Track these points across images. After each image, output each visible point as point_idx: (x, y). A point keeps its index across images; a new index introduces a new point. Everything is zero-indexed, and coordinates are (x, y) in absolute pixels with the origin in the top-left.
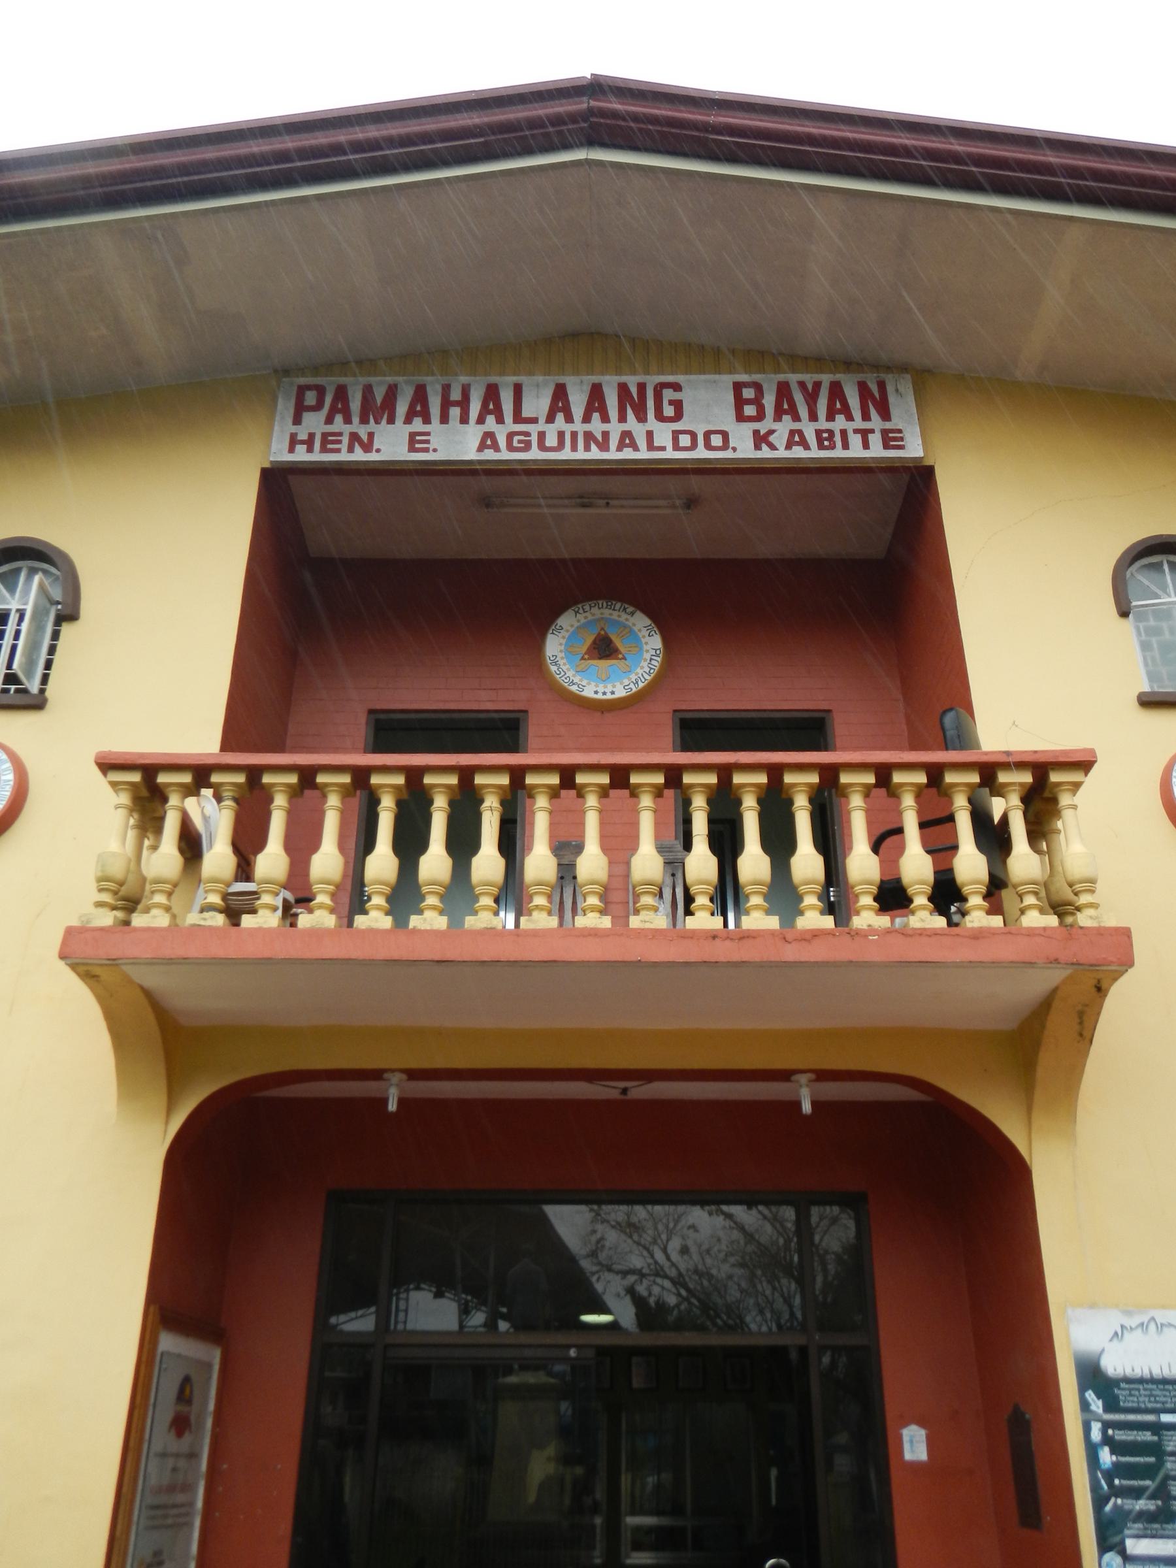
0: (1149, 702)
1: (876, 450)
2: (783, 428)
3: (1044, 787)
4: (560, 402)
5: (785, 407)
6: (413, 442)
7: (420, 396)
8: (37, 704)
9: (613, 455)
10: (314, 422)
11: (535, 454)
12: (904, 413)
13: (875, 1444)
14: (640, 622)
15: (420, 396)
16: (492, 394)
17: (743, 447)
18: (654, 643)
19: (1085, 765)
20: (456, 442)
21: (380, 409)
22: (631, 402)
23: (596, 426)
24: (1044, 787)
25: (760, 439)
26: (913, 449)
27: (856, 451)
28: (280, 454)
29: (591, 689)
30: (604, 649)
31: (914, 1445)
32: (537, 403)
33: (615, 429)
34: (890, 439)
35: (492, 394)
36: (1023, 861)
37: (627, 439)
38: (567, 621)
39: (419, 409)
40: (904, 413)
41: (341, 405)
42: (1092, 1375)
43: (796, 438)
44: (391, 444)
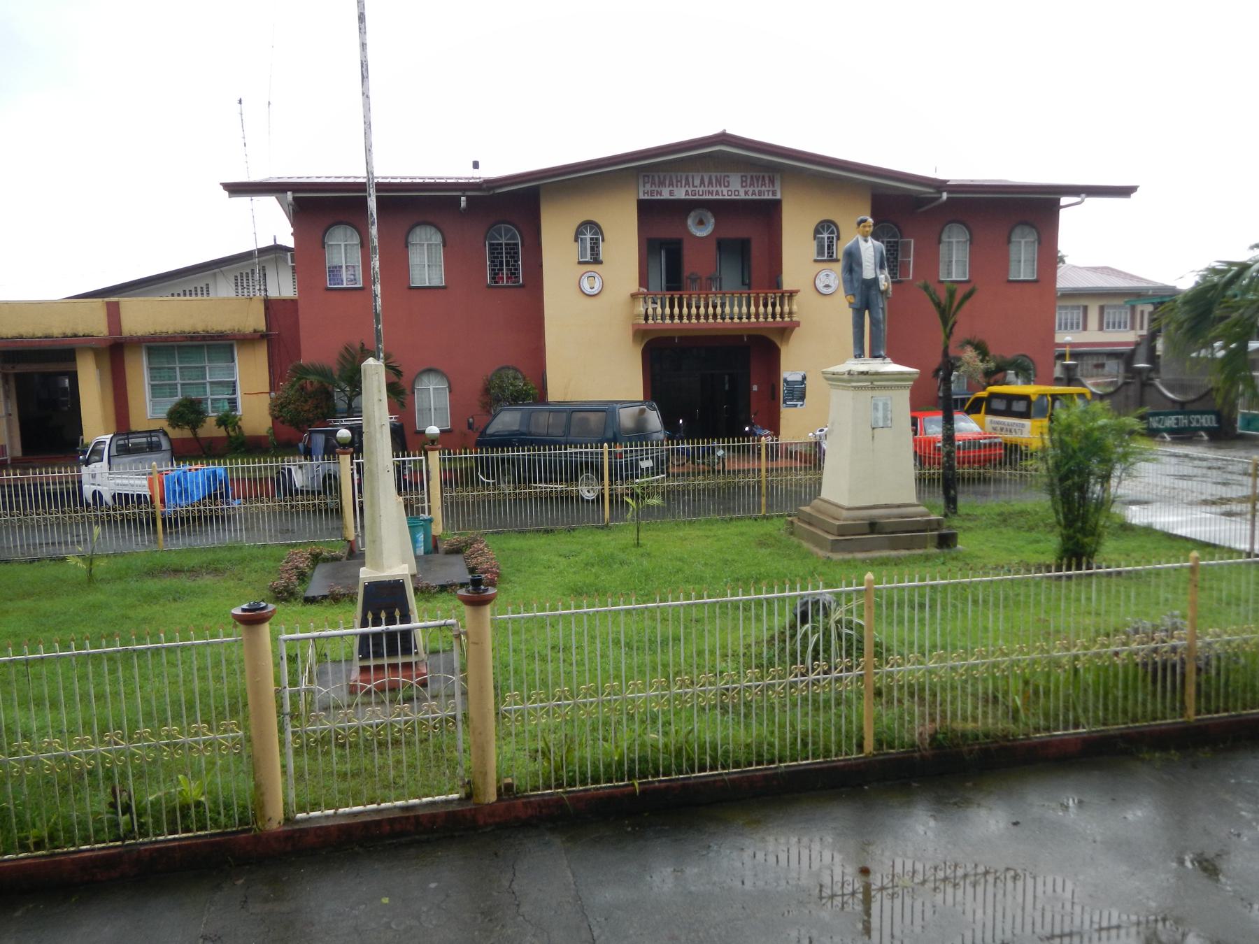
0: (816, 261)
1: (771, 197)
2: (751, 190)
3: (792, 294)
4: (702, 182)
5: (752, 184)
6: (671, 193)
7: (671, 180)
8: (601, 263)
9: (715, 197)
10: (648, 187)
11: (697, 197)
12: (778, 187)
13: (750, 388)
14: (709, 214)
15: (671, 180)
16: (687, 179)
17: (742, 196)
18: (713, 220)
19: (797, 292)
20: (680, 194)
21: (662, 184)
22: (719, 182)
23: (711, 189)
24: (792, 294)
25: (746, 193)
26: (778, 197)
27: (766, 197)
28: (642, 197)
29: (699, 234)
30: (701, 223)
31: (755, 388)
32: (697, 182)
33: (715, 189)
34: (774, 193)
35: (687, 179)
36: (786, 309)
37: (717, 193)
38: (692, 214)
39: (671, 184)
40: (778, 187)
41: (653, 183)
42: (785, 381)
43: (754, 193)
44: (665, 195)
